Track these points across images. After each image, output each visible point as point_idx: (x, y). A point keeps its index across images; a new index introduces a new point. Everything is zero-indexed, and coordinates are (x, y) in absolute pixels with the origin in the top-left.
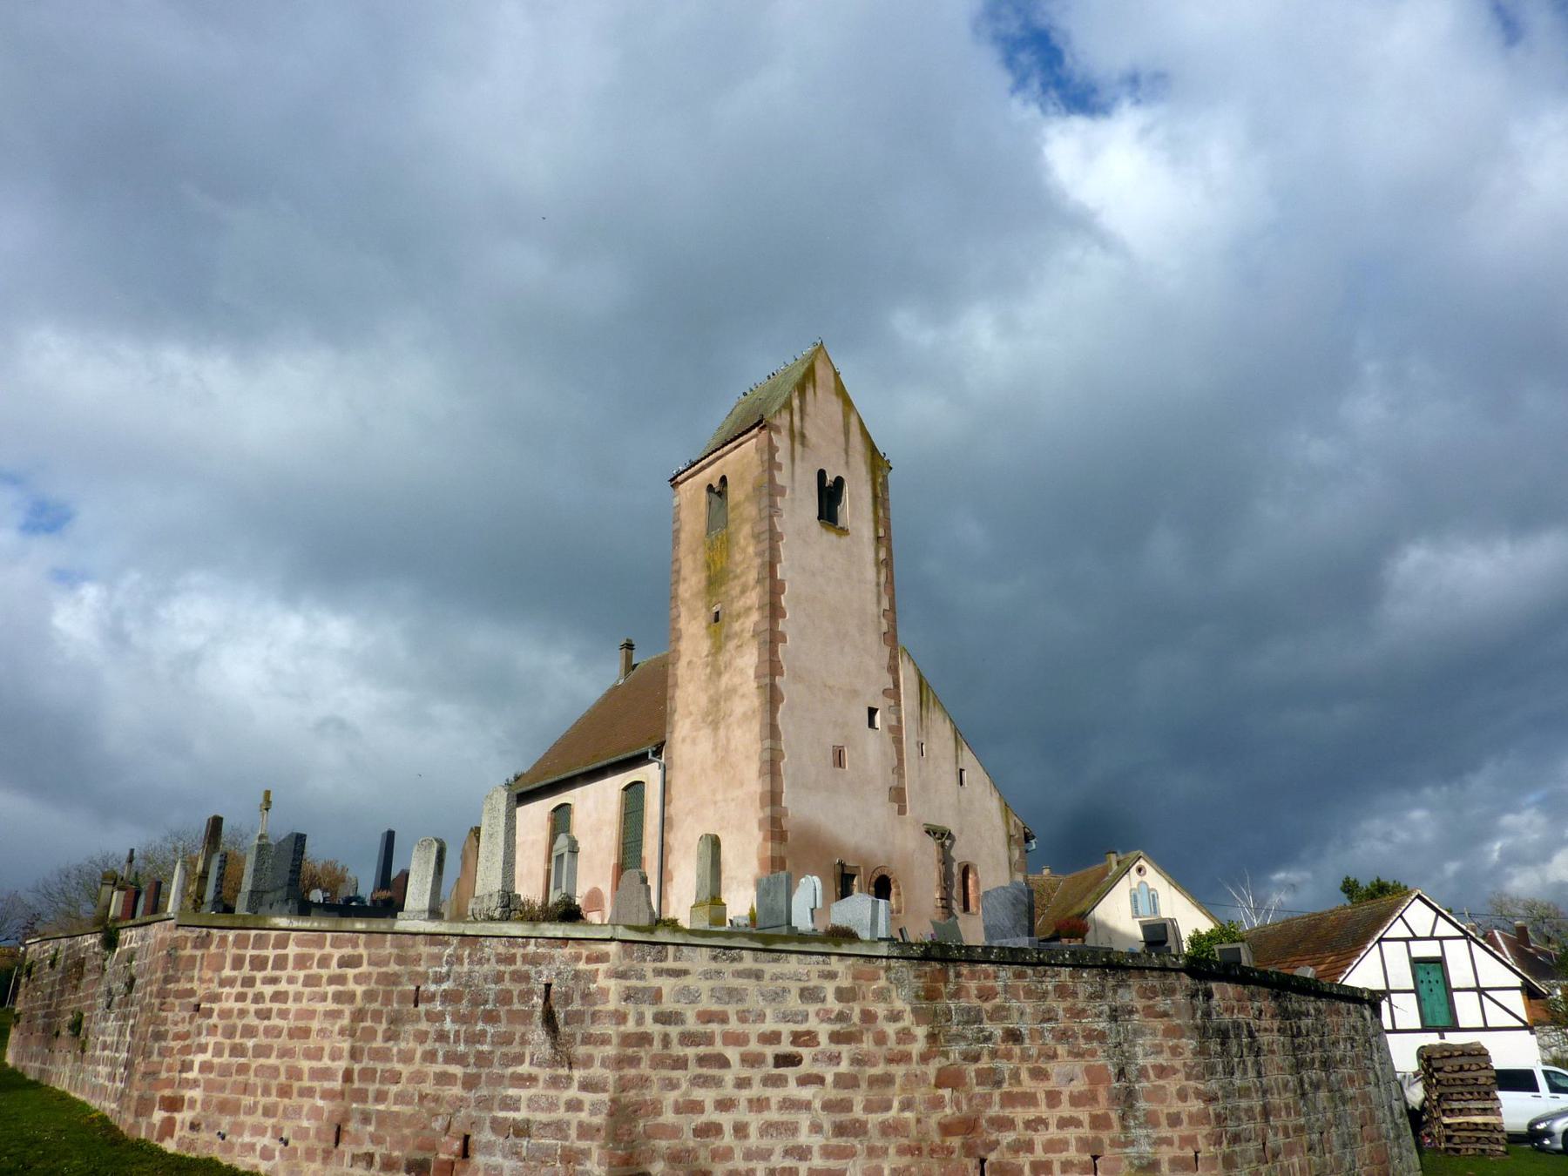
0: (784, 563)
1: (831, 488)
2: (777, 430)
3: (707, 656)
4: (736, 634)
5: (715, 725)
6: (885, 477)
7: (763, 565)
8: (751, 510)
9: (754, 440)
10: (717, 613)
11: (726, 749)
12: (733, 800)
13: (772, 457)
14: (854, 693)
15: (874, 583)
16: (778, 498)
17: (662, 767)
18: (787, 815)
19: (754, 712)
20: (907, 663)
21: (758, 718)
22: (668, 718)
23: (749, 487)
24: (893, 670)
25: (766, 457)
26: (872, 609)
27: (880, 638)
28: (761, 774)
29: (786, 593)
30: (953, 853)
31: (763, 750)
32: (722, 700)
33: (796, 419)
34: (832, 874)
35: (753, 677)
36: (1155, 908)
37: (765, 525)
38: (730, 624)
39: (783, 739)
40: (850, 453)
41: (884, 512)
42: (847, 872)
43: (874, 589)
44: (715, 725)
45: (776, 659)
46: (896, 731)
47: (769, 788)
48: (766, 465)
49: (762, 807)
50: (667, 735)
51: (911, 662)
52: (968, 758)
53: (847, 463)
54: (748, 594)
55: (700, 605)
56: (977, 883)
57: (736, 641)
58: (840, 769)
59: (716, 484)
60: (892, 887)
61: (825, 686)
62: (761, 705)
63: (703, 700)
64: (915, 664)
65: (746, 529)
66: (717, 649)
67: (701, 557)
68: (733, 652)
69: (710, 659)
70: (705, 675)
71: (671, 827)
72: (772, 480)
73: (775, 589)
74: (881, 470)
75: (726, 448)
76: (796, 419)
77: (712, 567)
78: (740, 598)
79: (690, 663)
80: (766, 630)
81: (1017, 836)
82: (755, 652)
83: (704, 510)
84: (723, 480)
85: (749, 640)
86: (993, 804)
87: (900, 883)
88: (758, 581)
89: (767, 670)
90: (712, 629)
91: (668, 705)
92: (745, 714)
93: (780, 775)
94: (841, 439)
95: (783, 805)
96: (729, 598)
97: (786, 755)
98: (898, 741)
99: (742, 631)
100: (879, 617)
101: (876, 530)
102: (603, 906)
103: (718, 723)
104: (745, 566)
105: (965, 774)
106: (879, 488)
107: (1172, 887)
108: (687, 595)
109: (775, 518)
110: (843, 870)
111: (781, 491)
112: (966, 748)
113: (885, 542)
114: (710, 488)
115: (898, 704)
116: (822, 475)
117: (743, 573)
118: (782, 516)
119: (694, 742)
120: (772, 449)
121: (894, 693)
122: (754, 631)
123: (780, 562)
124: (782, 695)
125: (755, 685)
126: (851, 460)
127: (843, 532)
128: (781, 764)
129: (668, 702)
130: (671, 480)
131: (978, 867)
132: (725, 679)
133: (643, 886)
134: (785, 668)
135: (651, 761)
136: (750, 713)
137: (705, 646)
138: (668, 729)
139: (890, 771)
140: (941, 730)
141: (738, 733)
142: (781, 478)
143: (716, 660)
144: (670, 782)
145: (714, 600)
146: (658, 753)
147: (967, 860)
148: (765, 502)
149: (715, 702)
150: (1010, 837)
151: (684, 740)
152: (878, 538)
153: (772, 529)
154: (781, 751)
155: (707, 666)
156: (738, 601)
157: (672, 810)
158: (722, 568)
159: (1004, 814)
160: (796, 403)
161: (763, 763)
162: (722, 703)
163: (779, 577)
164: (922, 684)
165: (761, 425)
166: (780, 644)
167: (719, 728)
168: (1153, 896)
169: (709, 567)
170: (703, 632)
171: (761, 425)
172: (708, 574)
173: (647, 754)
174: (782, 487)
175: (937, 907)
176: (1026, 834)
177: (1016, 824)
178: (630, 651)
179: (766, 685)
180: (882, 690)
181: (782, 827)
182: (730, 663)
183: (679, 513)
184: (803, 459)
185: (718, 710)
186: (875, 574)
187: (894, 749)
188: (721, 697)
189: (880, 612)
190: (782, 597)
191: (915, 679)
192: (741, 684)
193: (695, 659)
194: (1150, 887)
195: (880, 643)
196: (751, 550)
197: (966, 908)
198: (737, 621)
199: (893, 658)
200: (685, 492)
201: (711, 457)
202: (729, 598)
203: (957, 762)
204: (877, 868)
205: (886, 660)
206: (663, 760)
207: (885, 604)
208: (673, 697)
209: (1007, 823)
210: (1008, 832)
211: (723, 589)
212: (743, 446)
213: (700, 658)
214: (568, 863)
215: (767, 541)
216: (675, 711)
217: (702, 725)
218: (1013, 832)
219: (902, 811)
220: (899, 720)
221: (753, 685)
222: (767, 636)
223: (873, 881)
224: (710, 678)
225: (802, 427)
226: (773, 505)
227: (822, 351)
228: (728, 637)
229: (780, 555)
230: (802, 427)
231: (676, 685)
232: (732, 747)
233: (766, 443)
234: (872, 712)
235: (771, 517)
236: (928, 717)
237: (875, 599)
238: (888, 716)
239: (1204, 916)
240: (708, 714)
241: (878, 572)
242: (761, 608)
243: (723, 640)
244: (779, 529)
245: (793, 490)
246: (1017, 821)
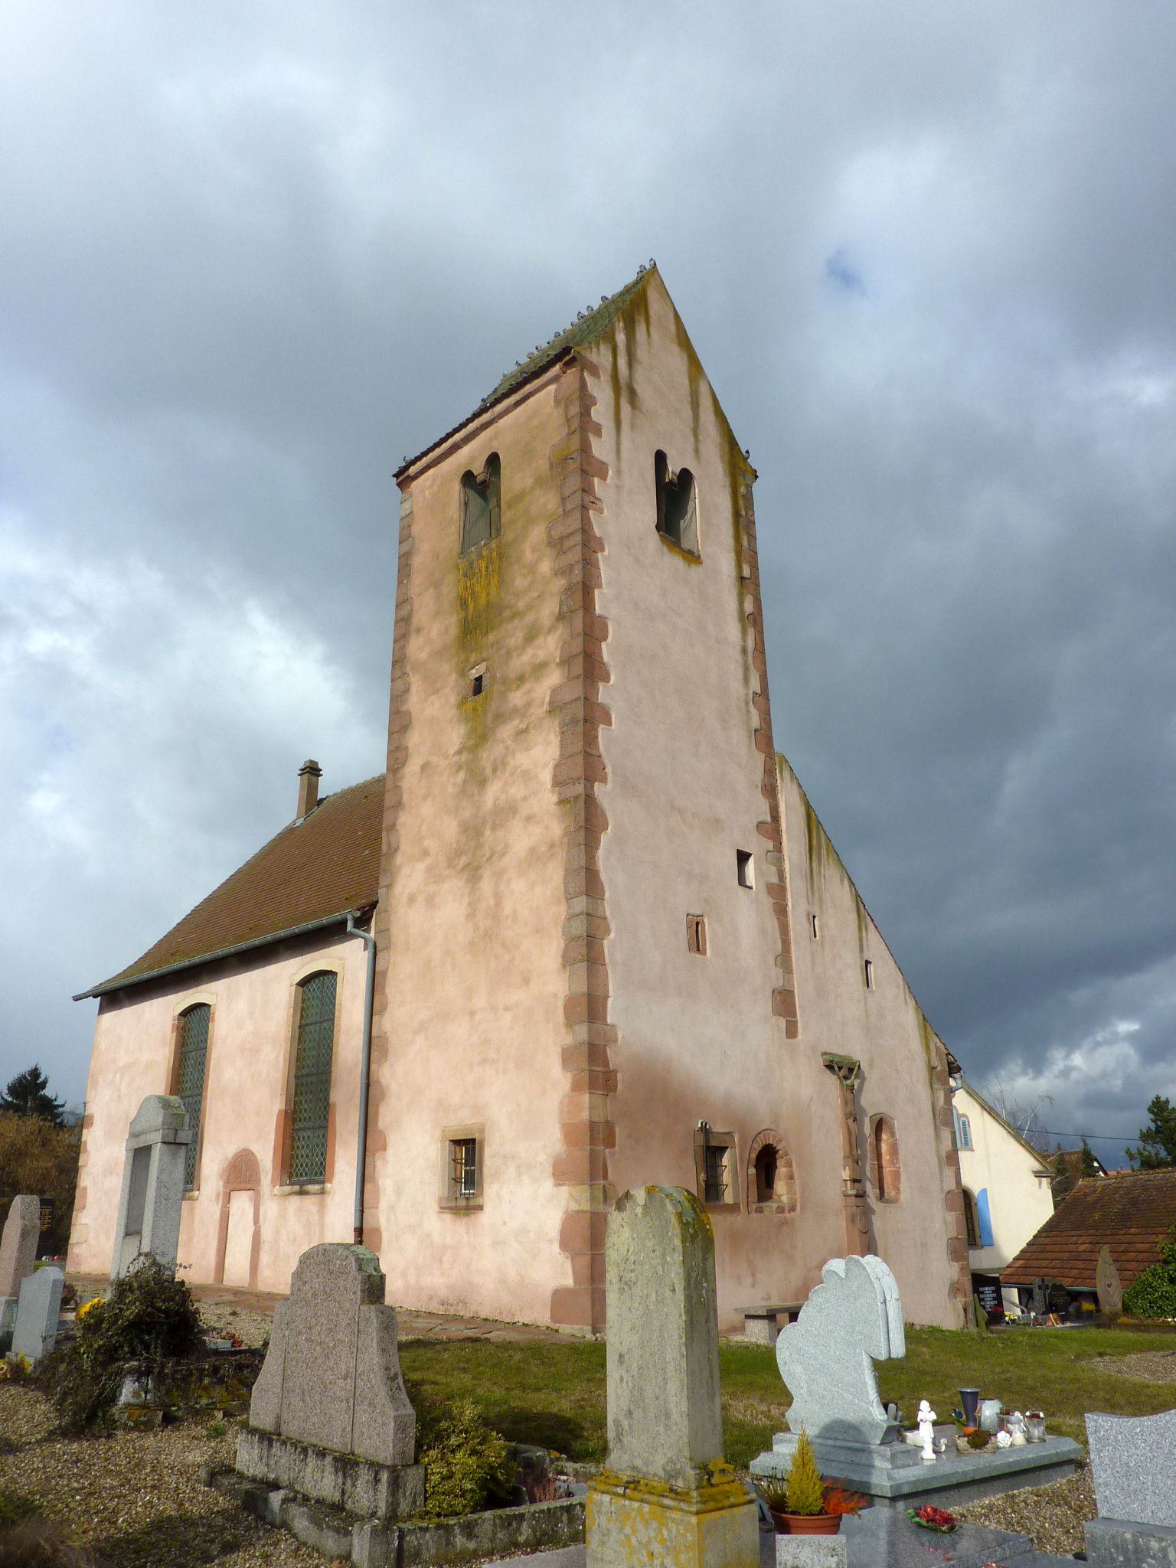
0: (605, 590)
1: (675, 485)
2: (595, 371)
3: (459, 752)
4: (516, 711)
5: (473, 873)
6: (749, 487)
7: (569, 590)
8: (547, 501)
9: (552, 388)
10: (479, 679)
11: (495, 915)
12: (506, 1009)
13: (585, 412)
14: (716, 824)
15: (738, 648)
16: (596, 480)
17: (370, 946)
18: (616, 1041)
19: (552, 846)
20: (789, 784)
21: (561, 855)
22: (383, 863)
23: (542, 464)
24: (770, 791)
25: (575, 409)
26: (736, 687)
27: (750, 737)
28: (567, 961)
29: (609, 639)
30: (863, 1102)
31: (570, 918)
32: (489, 825)
33: (622, 362)
35: (549, 785)
36: (966, 1139)
37: (575, 522)
38: (503, 695)
39: (607, 895)
40: (700, 438)
41: (748, 539)
42: (713, 1143)
43: (738, 656)
44: (473, 873)
45: (594, 752)
46: (777, 892)
47: (583, 988)
48: (575, 424)
49: (570, 1024)
50: (382, 892)
51: (795, 782)
52: (873, 938)
53: (697, 451)
54: (540, 641)
55: (447, 669)
56: (894, 1149)
57: (516, 722)
58: (699, 956)
59: (478, 468)
60: (779, 1163)
61: (673, 807)
62: (567, 833)
63: (450, 828)
64: (800, 786)
65: (537, 533)
66: (479, 737)
67: (450, 588)
68: (509, 742)
69: (464, 757)
70: (454, 785)
71: (385, 1053)
72: (585, 449)
73: (592, 631)
74: (744, 475)
75: (499, 408)
76: (622, 362)
77: (471, 606)
78: (523, 649)
79: (425, 767)
80: (577, 699)
81: (939, 1069)
82: (555, 740)
83: (456, 516)
84: (493, 461)
85: (541, 719)
86: (908, 1017)
87: (793, 1157)
88: (561, 617)
89: (579, 771)
90: (470, 705)
91: (384, 841)
92: (532, 850)
94: (687, 412)
95: (609, 1021)
96: (503, 652)
97: (613, 926)
98: (781, 911)
99: (529, 704)
100: (747, 703)
101: (739, 566)
102: (258, 1181)
103: (479, 867)
104: (535, 594)
105: (872, 968)
106: (741, 502)
107: (985, 1113)
108: (423, 655)
109: (591, 512)
110: (707, 1140)
111: (602, 471)
112: (871, 927)
113: (751, 587)
114: (468, 478)
115: (778, 848)
116: (660, 458)
117: (529, 608)
118: (601, 511)
119: (431, 901)
120: (586, 402)
121: (771, 829)
122: (551, 703)
123: (600, 586)
124: (604, 815)
125: (554, 798)
126: (702, 449)
127: (692, 557)
128: (605, 942)
129: (384, 834)
130: (396, 476)
131: (895, 1122)
132: (493, 792)
133: (370, 1311)
134: (609, 769)
135: (353, 936)
136: (543, 849)
137: (455, 736)
138: (383, 881)
140: (839, 895)
141: (519, 885)
142: (601, 448)
144: (384, 973)
145: (473, 657)
146: (363, 922)
147: (882, 1111)
148: (574, 483)
149: (473, 831)
150: (932, 1069)
151: (412, 899)
152: (742, 579)
153: (586, 528)
155: (459, 768)
156: (519, 655)
157: (386, 1023)
158: (488, 603)
159: (922, 1032)
160: (621, 338)
161: (570, 940)
162: (487, 833)
163: (598, 610)
164: (811, 820)
165: (567, 358)
166: (601, 726)
168: (964, 1123)
169: (463, 604)
170: (452, 712)
171: (567, 358)
172: (463, 615)
173: (344, 922)
174: (603, 463)
175: (846, 1196)
176: (950, 1064)
177: (937, 1048)
178: (314, 778)
179: (576, 798)
181: (607, 1064)
182: (504, 763)
183: (409, 526)
184: (633, 426)
185: (480, 846)
186: (739, 634)
188: (484, 823)
189: (747, 694)
190: (604, 645)
191: (801, 810)
192: (525, 799)
193: (435, 760)
194: (960, 1112)
195: (750, 744)
196: (545, 567)
197: (882, 1195)
198: (518, 687)
199: (769, 772)
200: (423, 491)
201: (471, 427)
202: (503, 652)
204: (760, 1133)
205: (758, 776)
206: (372, 934)
207: (755, 685)
208: (392, 827)
209: (928, 1048)
210: (929, 1062)
211: (491, 637)
212: (531, 400)
213: (446, 757)
214: (161, 1171)
215: (579, 548)
216: (396, 850)
218: (935, 1062)
219: (791, 1032)
221: (548, 798)
222: (579, 710)
225: (631, 376)
226: (587, 490)
227: (656, 276)
228: (500, 718)
229: (599, 576)
230: (631, 376)
232: (507, 909)
233: (577, 385)
234: (743, 857)
235: (584, 508)
236: (820, 872)
237: (740, 673)
238: (765, 867)
239: (1021, 1147)
240: (458, 853)
241: (744, 633)
242: (566, 662)
243: (489, 721)
244: (597, 531)
245: (619, 472)
246: (939, 1044)
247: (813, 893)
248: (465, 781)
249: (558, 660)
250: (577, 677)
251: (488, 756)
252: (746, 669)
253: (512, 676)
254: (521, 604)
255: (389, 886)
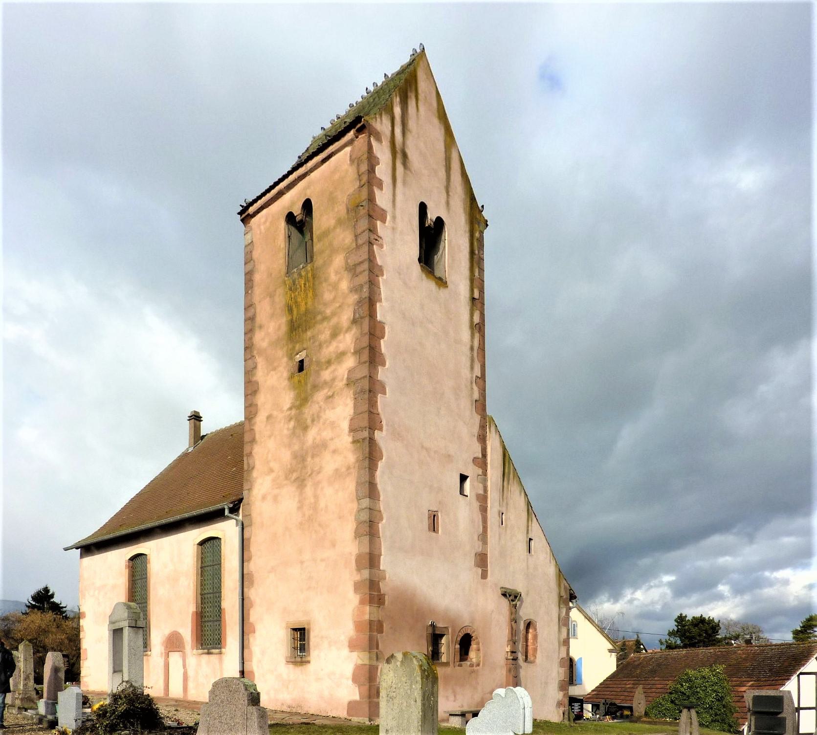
3: (290, 409)
4: (326, 383)
5: (301, 483)
10: (302, 362)
32: (310, 454)
44: (301, 483)
54: (341, 337)
63: (286, 456)
66: (302, 400)
69: (293, 412)
70: (288, 429)
78: (330, 342)
88: (354, 321)
90: (296, 379)
96: (317, 344)
99: (334, 380)
104: (337, 305)
117: (334, 314)
123: (380, 301)
125: (350, 439)
129: (245, 458)
130: (240, 213)
132: (312, 435)
137: (287, 398)
143: (301, 413)
149: (300, 458)
162: (309, 459)
167: (305, 486)
169: (290, 310)
182: (319, 417)
198: (327, 368)
202: (317, 344)
211: (309, 333)
217: (285, 482)
224: (294, 433)
228: (316, 387)
231: (253, 441)
242: (357, 352)
248: (294, 428)
249: (352, 351)
250: (365, 362)
251: (309, 411)
253: (323, 360)
254: (328, 312)
255: (250, 490)
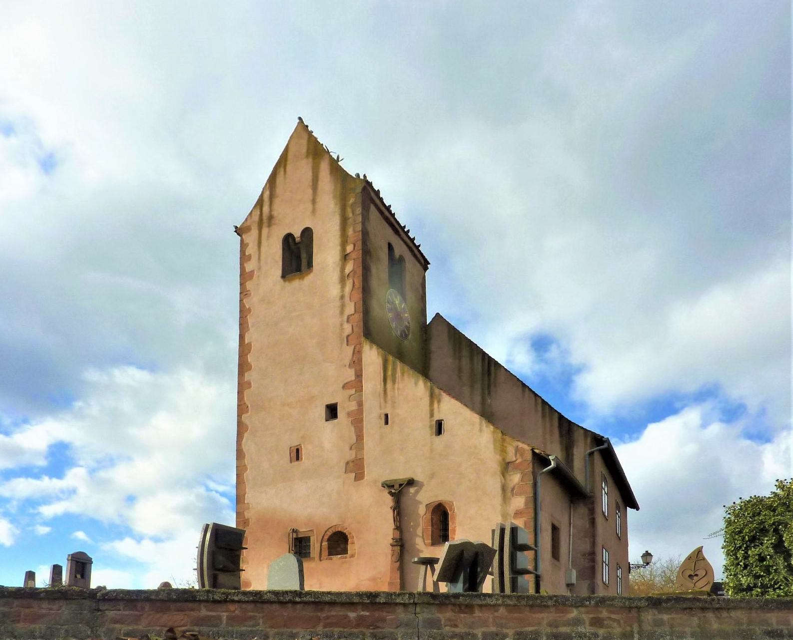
14: (312, 399)
30: (419, 497)
34: (286, 540)
53: (314, 211)
87: (354, 534)
93: (244, 483)
95: (246, 502)
128: (245, 475)
131: (454, 503)
139: (347, 448)
154: (245, 465)
180: (341, 386)
187: (353, 429)
203: (432, 415)
220: (360, 404)
223: (326, 537)
225: (271, 211)
236: (394, 389)
247: (386, 402)
252: (343, 307)
